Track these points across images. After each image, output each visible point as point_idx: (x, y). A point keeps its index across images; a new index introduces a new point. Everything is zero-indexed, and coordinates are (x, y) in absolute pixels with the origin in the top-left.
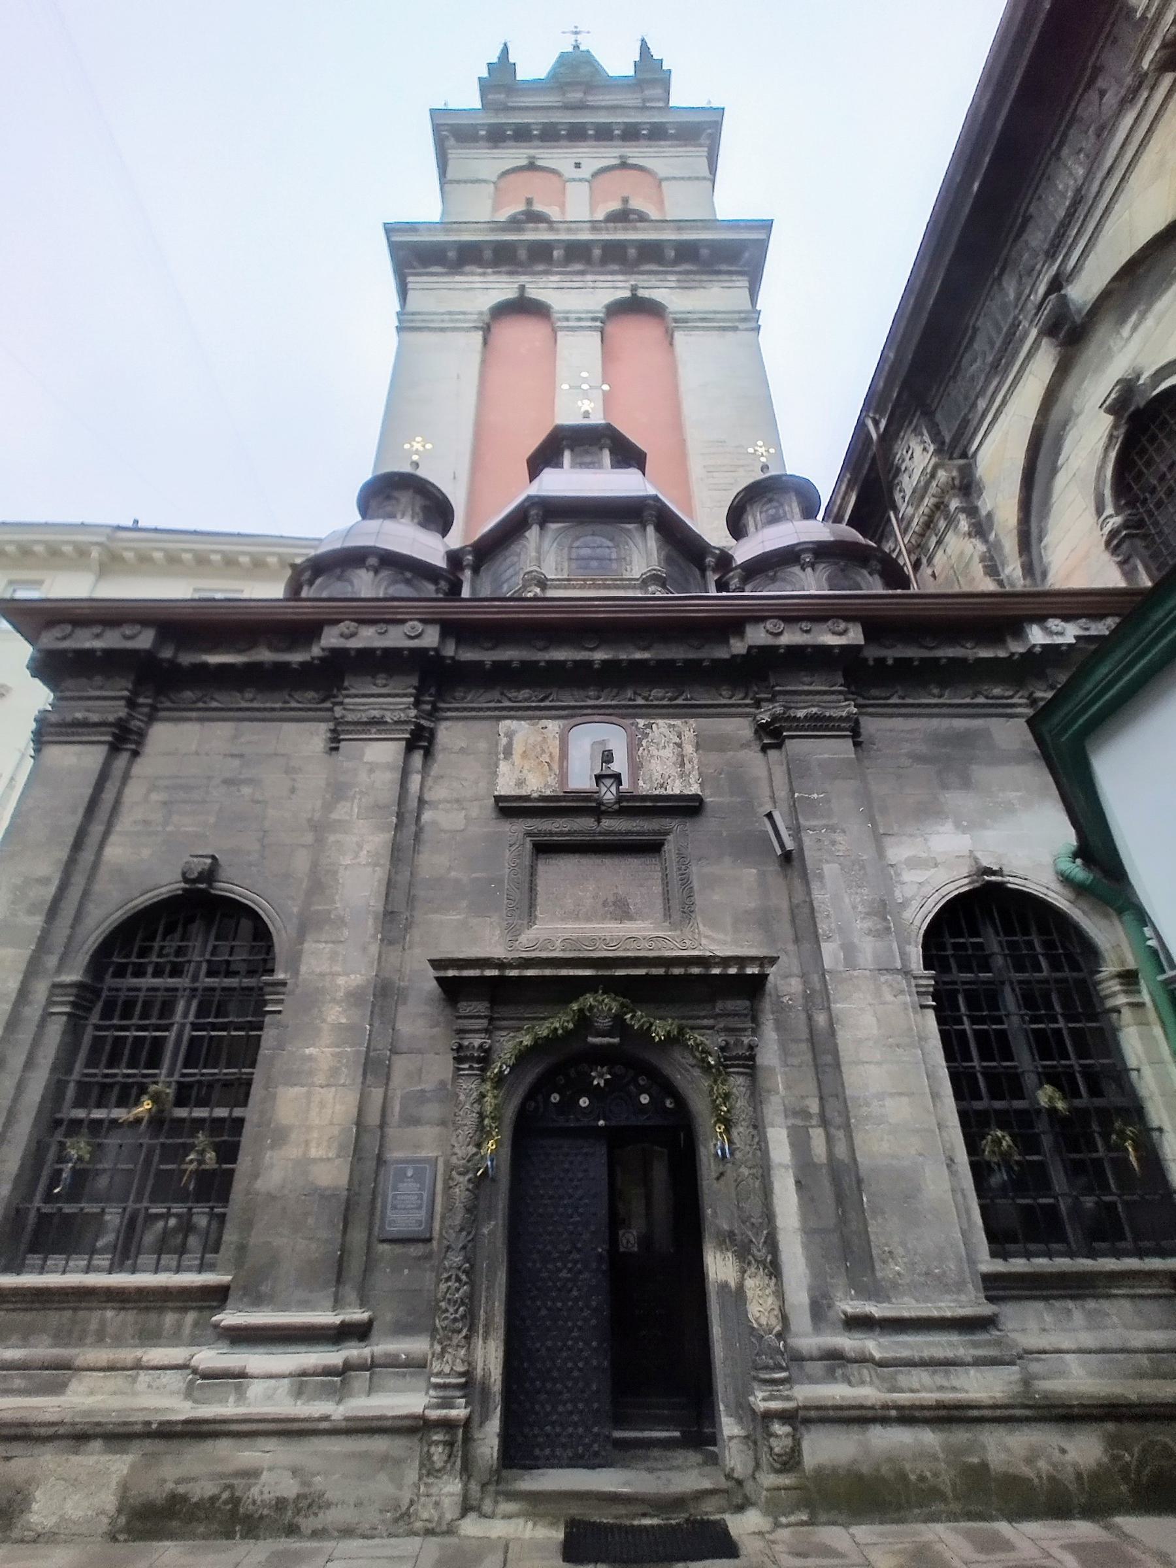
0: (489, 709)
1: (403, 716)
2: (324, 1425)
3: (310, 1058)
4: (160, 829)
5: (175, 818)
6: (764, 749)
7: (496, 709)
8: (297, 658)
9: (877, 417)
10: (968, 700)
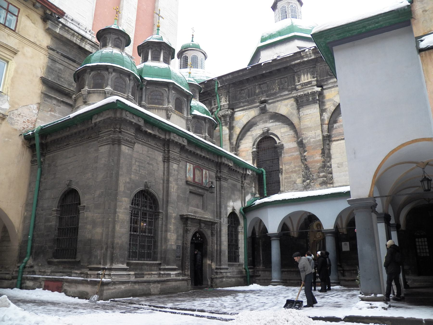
0: (185, 159)
1: (178, 159)
2: (179, 280)
3: (171, 228)
4: (139, 172)
5: (141, 170)
6: (216, 181)
7: (186, 159)
8: (163, 137)
9: (219, 83)
10: (236, 178)
